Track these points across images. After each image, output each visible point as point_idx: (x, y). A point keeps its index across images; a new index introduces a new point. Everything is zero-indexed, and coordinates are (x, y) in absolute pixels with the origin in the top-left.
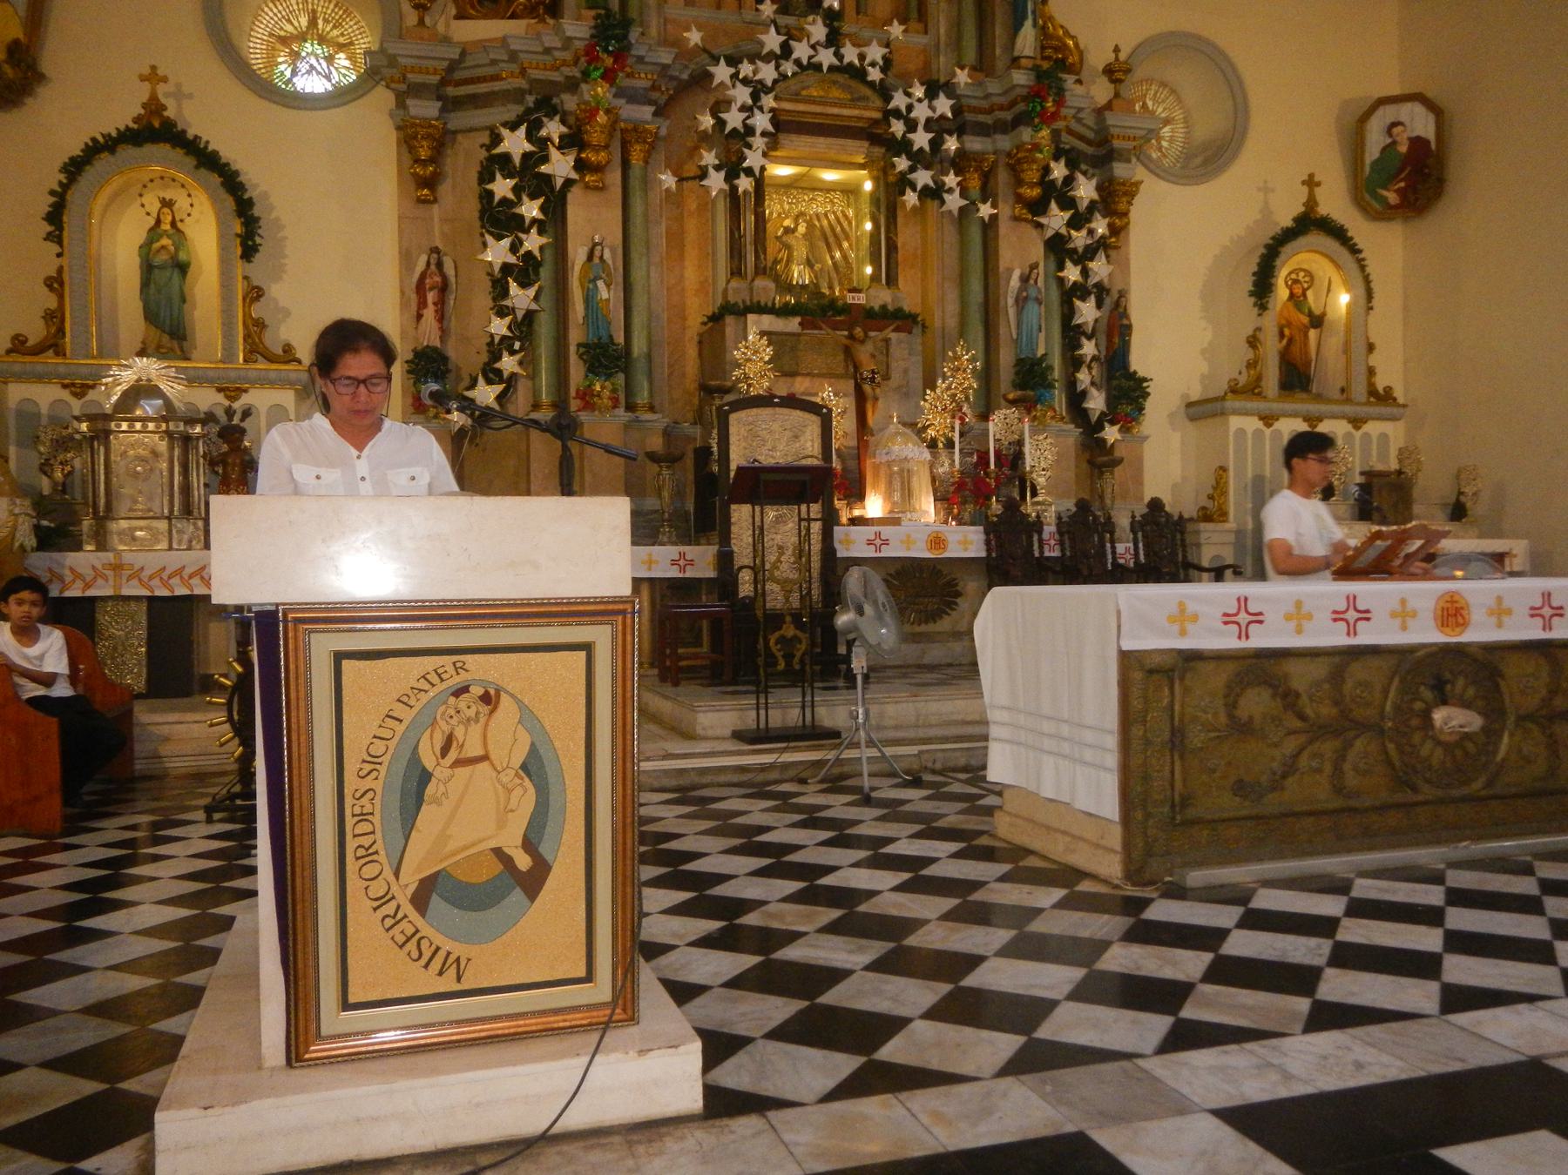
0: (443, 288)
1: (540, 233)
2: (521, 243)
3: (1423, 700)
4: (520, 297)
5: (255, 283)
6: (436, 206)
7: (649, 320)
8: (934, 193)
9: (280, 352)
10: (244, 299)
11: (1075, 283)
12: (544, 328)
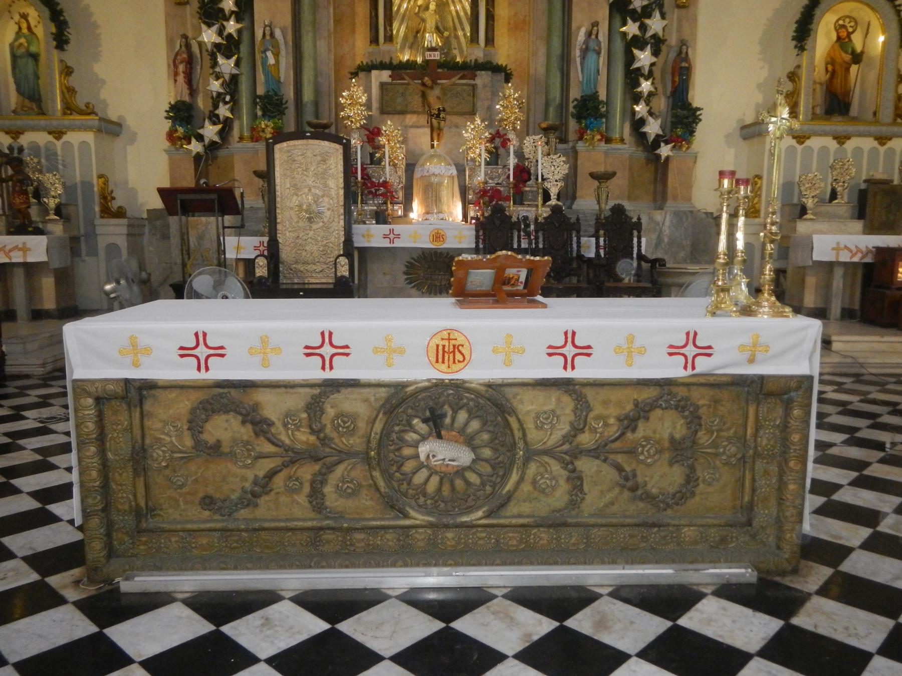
0: (190, 61)
1: (238, 21)
2: (224, 27)
3: (415, 432)
4: (226, 65)
5: (69, 64)
6: (188, 6)
7: (316, 76)
9: (84, 108)
10: (61, 74)
11: (635, 37)
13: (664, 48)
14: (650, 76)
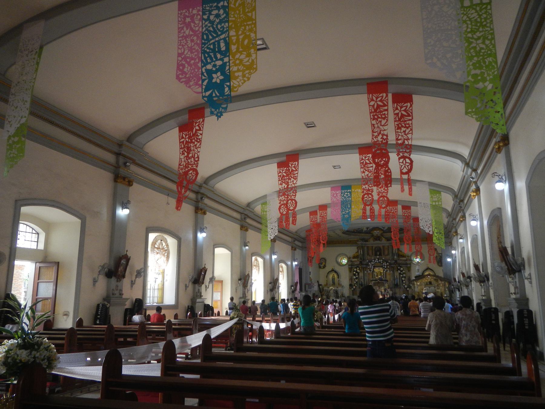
8: (387, 271)
12: (358, 282)
13: (406, 277)
14: (405, 280)
